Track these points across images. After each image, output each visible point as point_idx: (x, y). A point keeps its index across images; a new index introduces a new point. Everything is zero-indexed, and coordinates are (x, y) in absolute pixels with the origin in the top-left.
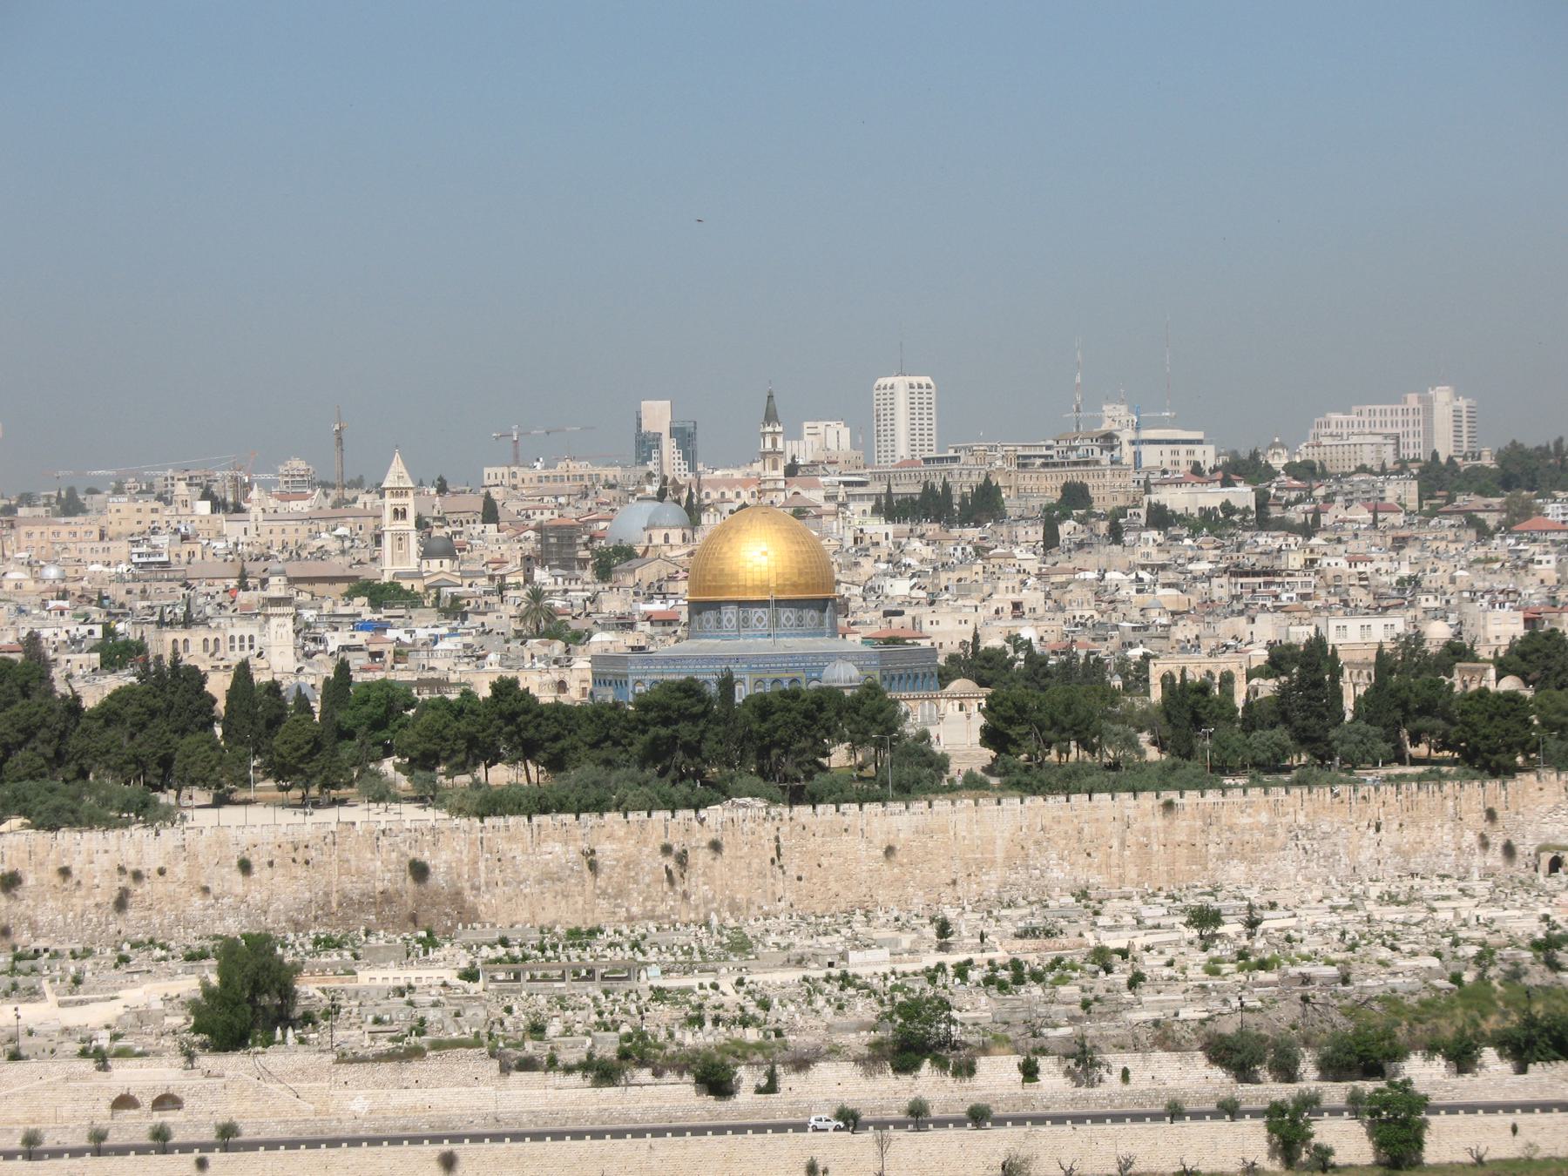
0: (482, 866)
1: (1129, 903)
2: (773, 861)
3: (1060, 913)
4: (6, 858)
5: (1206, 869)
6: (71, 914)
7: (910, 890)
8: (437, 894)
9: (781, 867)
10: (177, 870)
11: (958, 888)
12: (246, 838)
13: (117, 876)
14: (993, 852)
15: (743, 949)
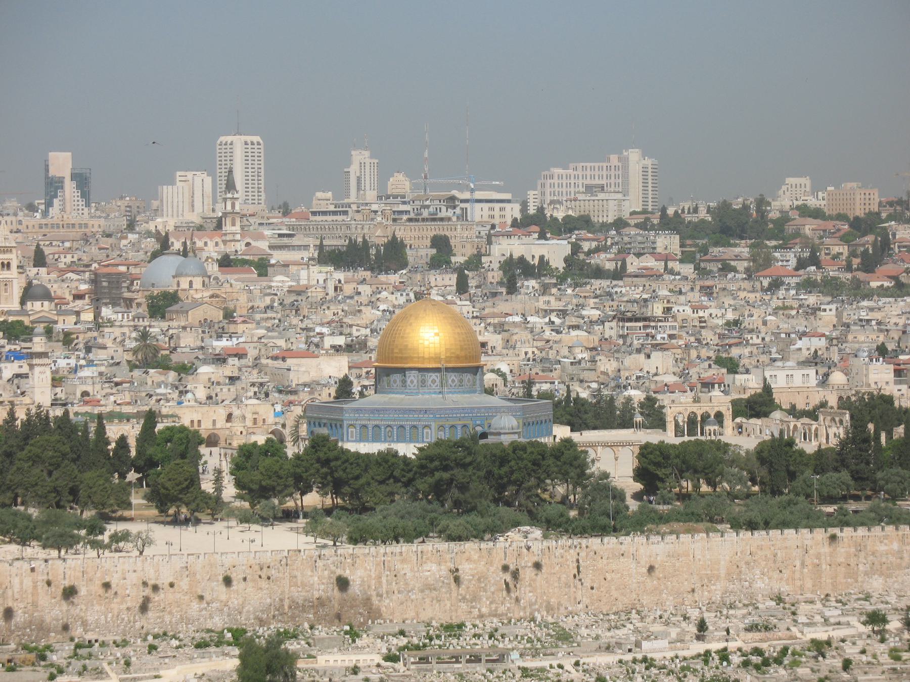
0: (384, 580)
1: (814, 607)
2: (575, 576)
3: (769, 613)
4: (67, 576)
5: (857, 581)
6: (110, 615)
7: (664, 595)
8: (354, 599)
9: (580, 580)
10: (181, 583)
11: (696, 595)
12: (228, 561)
13: (141, 588)
14: (718, 570)
15: (566, 639)
